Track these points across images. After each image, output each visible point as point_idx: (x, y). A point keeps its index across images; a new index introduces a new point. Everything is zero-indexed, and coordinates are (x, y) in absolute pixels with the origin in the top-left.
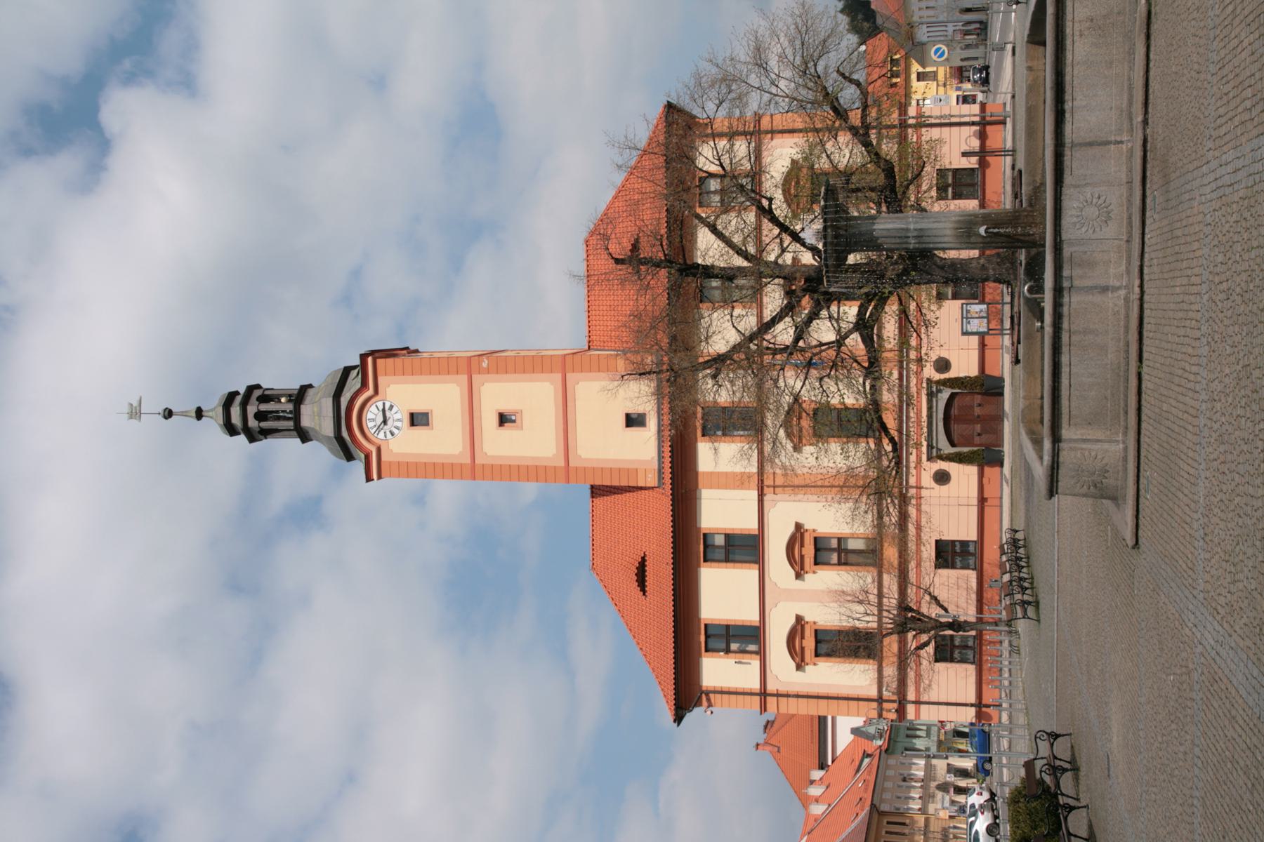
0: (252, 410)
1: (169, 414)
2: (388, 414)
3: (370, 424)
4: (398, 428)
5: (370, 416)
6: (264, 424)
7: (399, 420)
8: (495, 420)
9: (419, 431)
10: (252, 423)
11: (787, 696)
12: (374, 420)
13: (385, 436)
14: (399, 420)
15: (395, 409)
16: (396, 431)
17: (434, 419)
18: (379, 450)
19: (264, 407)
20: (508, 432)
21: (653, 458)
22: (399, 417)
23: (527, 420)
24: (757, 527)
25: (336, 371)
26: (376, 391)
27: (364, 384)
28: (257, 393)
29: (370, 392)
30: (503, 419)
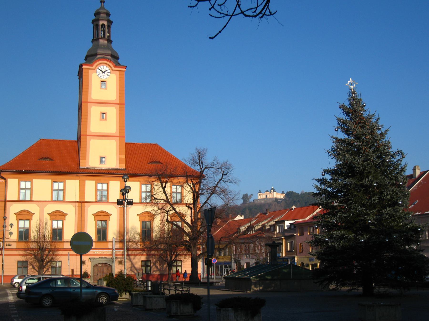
3: (102, 67)
5: (105, 67)
7: (103, 77)
11: (5, 209)
13: (98, 72)
14: (103, 77)
15: (107, 76)
16: (99, 76)
18: (94, 69)
20: (98, 115)
21: (90, 165)
22: (104, 77)
23: (103, 122)
24: (66, 200)
29: (114, 69)
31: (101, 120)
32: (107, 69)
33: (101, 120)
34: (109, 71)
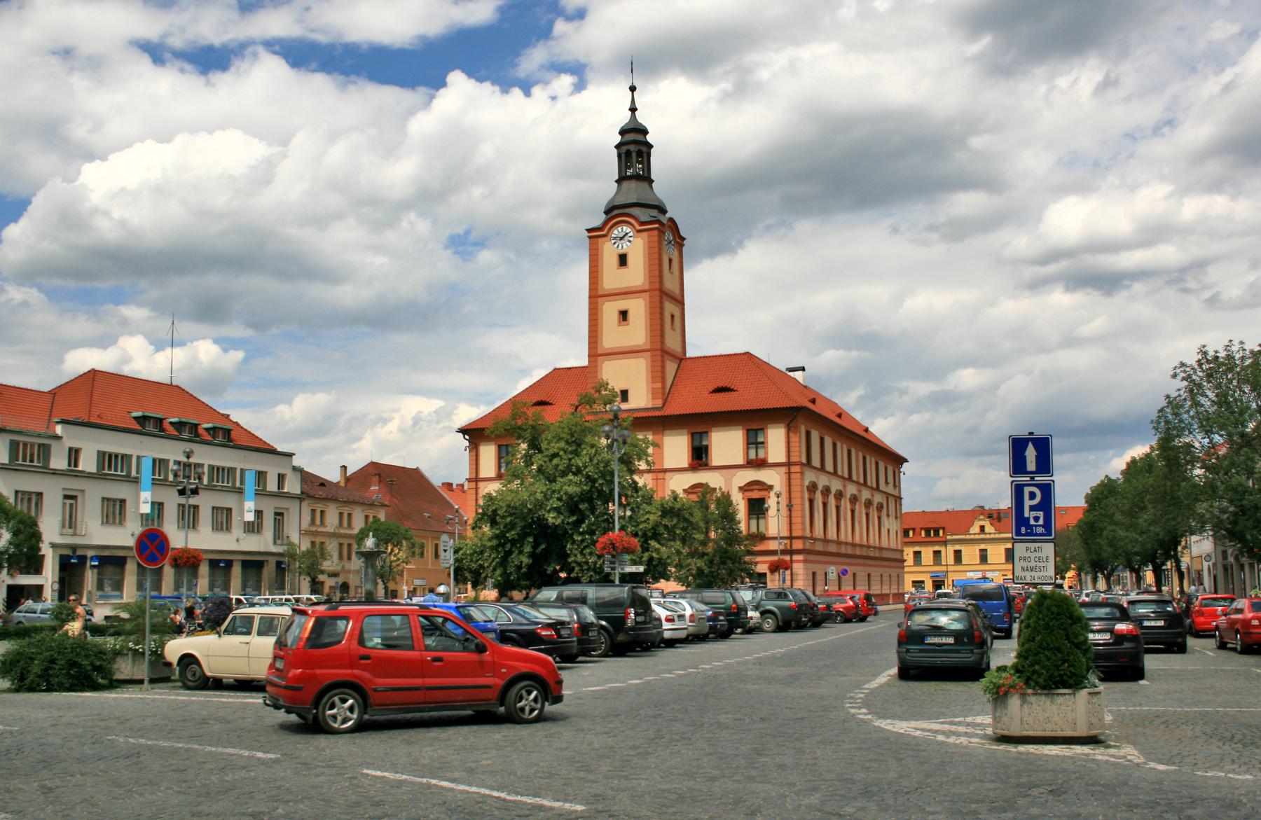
0: (632, 148)
1: (633, 89)
2: (626, 238)
3: (620, 229)
4: (618, 247)
5: (625, 228)
6: (623, 155)
8: (623, 308)
9: (615, 260)
10: (624, 149)
12: (622, 229)
15: (629, 244)
17: (623, 270)
19: (634, 155)
20: (616, 316)
22: (625, 247)
26: (639, 231)
27: (642, 223)
28: (644, 149)
30: (624, 315)
31: (619, 324)
32: (629, 230)
33: (619, 324)
34: (631, 234)
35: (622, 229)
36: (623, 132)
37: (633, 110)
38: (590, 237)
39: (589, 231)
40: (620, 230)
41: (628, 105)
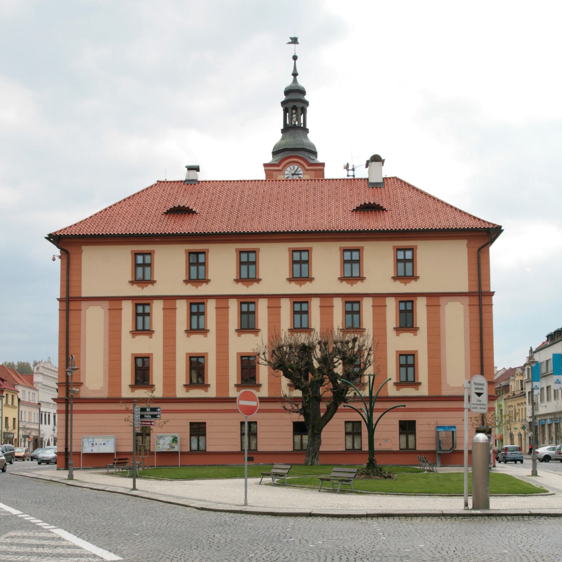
1: (295, 58)
3: (292, 167)
10: (291, 105)
13: (286, 175)
25: (316, 150)
29: (307, 167)
35: (294, 168)
36: (287, 92)
37: (295, 74)
38: (266, 170)
39: (265, 165)
40: (292, 168)
41: (292, 71)
